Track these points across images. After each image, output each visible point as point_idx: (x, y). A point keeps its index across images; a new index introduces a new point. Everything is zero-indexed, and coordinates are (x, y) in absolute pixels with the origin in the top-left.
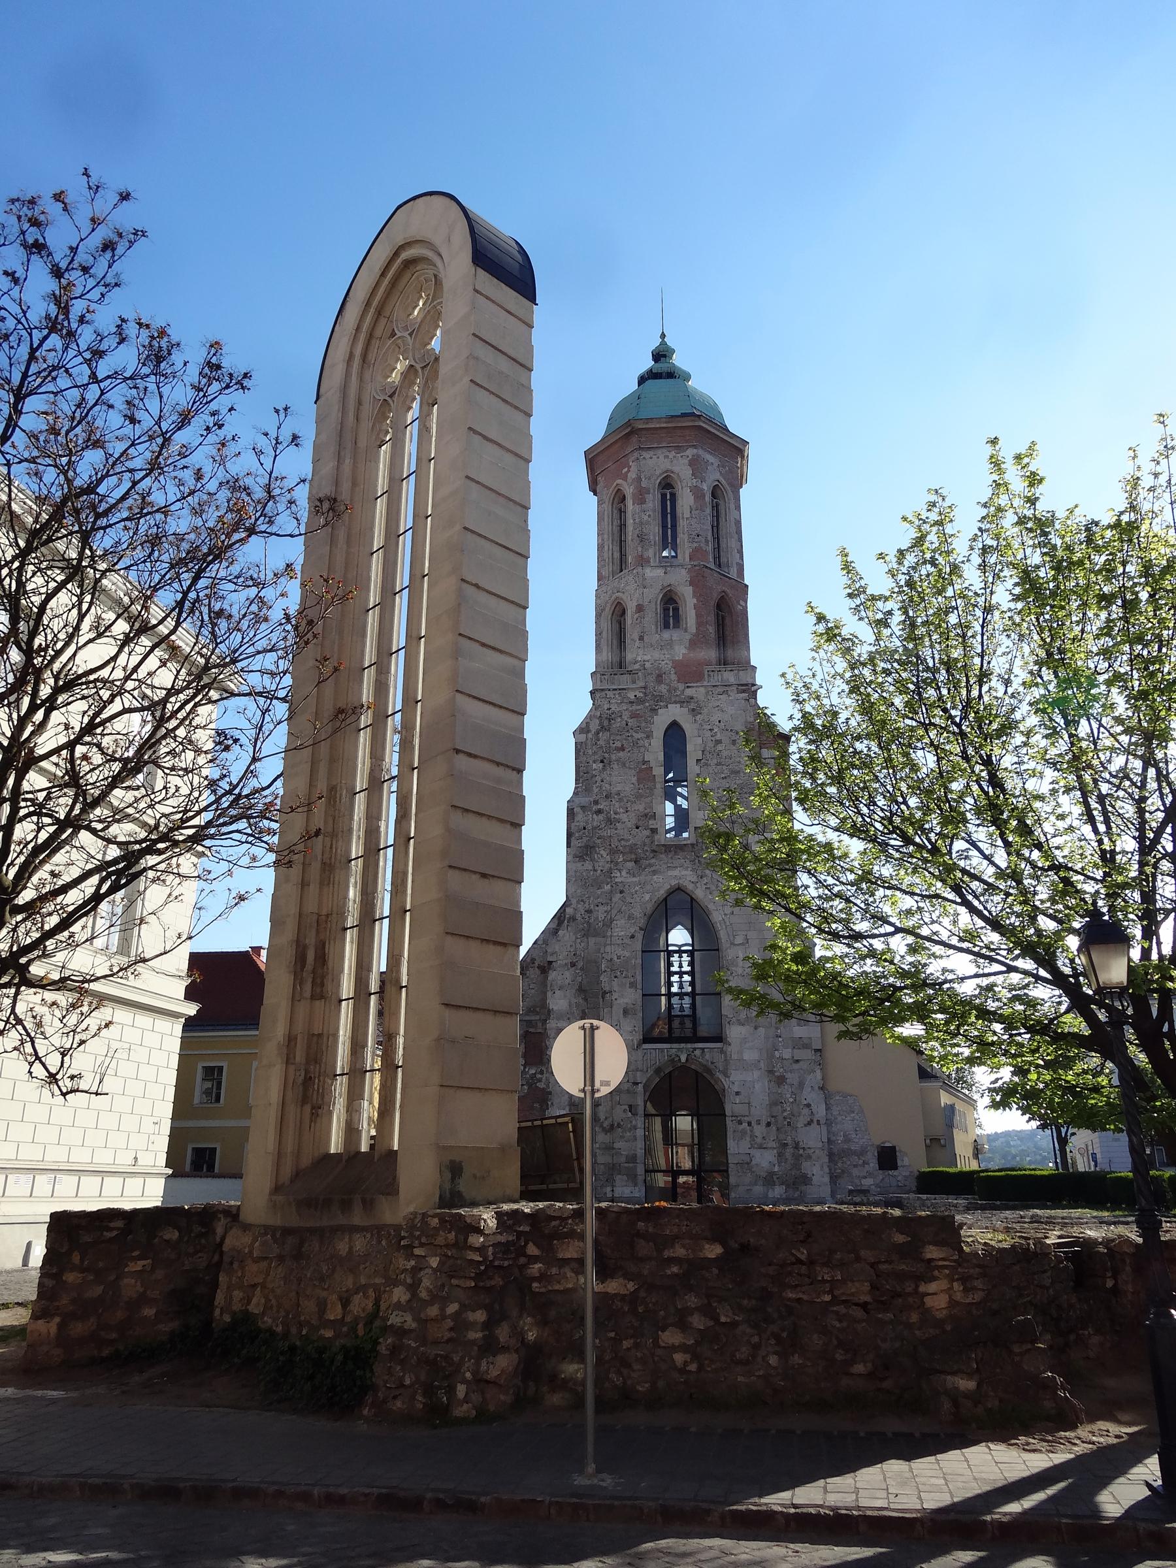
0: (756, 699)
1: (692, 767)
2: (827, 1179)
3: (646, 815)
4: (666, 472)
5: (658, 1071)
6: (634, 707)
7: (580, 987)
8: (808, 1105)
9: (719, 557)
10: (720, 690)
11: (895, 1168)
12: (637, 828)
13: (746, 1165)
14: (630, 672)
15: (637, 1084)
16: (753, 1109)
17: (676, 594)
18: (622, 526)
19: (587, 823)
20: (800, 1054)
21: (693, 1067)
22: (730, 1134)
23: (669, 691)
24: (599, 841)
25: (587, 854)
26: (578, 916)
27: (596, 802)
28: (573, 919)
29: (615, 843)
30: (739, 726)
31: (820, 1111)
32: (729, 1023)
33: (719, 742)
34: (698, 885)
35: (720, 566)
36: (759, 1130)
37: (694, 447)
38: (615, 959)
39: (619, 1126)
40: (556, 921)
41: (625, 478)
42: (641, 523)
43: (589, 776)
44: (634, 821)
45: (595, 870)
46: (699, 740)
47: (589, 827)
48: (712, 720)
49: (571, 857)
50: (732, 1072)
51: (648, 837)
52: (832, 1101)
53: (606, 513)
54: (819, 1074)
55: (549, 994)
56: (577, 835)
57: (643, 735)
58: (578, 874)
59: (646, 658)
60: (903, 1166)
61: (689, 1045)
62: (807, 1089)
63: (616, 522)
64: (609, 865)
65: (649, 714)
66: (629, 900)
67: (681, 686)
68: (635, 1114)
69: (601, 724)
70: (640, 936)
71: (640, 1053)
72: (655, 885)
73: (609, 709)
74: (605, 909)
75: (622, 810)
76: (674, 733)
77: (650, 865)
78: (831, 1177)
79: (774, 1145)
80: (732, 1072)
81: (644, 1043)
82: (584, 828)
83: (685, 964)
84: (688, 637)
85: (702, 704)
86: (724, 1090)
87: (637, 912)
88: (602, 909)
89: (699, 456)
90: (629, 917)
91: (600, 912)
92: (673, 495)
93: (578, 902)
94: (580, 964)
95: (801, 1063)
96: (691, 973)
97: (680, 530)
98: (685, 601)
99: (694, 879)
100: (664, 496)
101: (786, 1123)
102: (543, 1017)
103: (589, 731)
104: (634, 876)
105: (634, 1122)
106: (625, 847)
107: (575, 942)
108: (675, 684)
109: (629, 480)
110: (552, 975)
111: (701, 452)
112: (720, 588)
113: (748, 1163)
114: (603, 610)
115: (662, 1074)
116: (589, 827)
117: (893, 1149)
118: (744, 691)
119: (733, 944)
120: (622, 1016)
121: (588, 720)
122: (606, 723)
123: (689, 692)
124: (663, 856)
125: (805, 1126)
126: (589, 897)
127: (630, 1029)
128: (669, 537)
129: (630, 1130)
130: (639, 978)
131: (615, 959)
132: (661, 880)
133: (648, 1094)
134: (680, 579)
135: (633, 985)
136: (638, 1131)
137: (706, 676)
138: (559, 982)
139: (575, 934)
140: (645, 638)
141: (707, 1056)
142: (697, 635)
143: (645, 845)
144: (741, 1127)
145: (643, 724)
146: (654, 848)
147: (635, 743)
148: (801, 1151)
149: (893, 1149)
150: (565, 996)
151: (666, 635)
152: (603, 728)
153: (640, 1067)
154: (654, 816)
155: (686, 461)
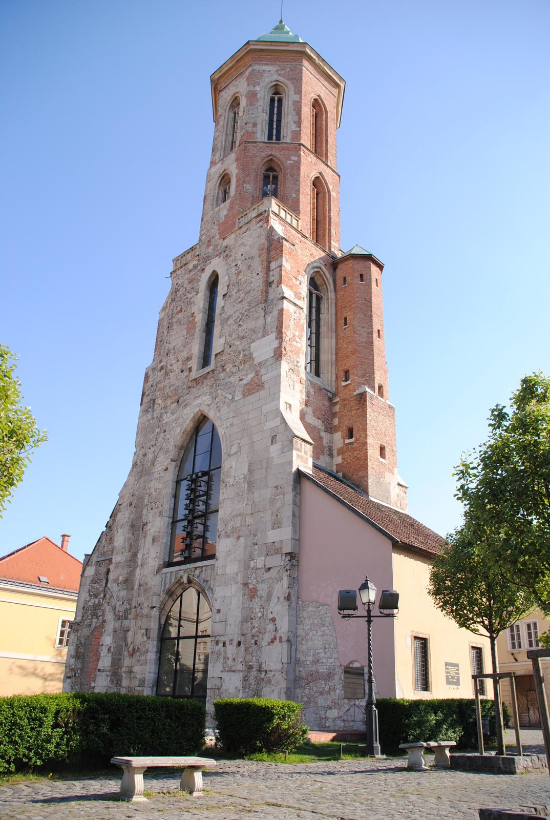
4: (235, 94)
8: (273, 620)
10: (244, 229)
23: (214, 250)
29: (167, 390)
30: (255, 252)
34: (212, 406)
36: (231, 650)
46: (227, 278)
48: (237, 256)
51: (187, 377)
52: (305, 614)
56: (147, 393)
61: (193, 565)
66: (168, 436)
70: (172, 467)
77: (184, 401)
82: (152, 386)
88: (153, 449)
93: (140, 450)
95: (271, 570)
99: (209, 403)
101: (253, 642)
105: (147, 646)
111: (256, 67)
112: (264, 154)
113: (219, 689)
120: (151, 544)
123: (225, 243)
124: (193, 390)
125: (269, 644)
135: (161, 513)
136: (149, 654)
146: (190, 384)
150: (123, 533)
152: (173, 300)
155: (245, 79)
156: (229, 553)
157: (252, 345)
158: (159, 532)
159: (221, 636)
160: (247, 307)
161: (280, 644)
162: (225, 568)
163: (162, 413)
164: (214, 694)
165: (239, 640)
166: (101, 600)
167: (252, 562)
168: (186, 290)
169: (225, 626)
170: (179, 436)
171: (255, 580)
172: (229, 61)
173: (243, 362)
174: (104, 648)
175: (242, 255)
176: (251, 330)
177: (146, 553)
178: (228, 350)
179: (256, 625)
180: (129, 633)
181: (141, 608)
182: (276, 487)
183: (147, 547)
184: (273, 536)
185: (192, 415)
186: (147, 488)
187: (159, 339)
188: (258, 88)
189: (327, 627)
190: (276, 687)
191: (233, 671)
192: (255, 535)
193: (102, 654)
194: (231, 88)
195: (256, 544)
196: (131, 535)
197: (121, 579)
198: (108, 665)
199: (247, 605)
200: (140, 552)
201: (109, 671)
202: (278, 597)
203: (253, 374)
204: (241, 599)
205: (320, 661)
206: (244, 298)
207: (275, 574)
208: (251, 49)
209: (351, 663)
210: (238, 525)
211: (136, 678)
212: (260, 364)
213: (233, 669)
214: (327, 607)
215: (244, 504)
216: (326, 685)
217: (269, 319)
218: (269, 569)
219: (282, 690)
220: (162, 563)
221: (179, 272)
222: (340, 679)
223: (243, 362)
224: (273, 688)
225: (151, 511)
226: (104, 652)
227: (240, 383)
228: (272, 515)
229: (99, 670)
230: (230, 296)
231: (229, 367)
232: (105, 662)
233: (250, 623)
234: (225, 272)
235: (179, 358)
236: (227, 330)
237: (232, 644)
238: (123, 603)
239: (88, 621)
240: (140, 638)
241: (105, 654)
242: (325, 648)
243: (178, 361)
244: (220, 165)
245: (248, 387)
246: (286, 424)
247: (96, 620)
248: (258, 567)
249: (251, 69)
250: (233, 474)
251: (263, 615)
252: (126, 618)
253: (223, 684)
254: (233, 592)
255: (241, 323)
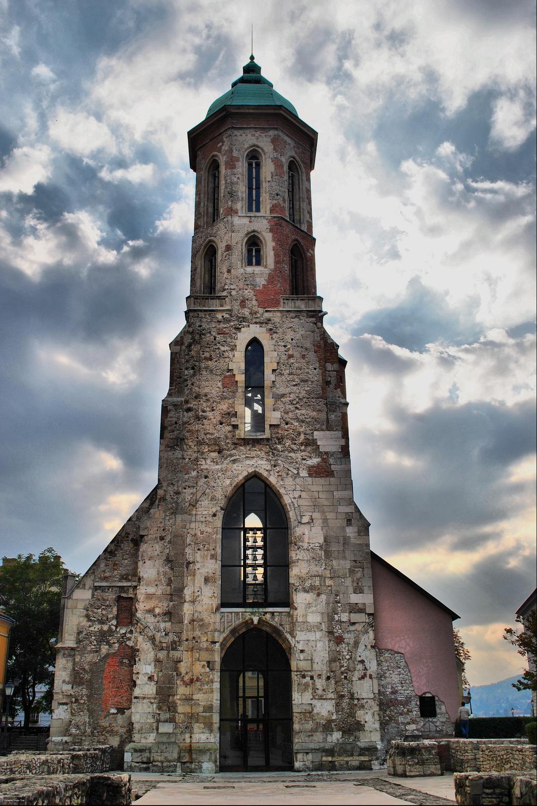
0: (322, 323)
1: (269, 377)
2: (377, 726)
3: (229, 414)
5: (233, 632)
6: (222, 325)
7: (167, 558)
8: (362, 662)
9: (293, 215)
11: (434, 714)
12: (221, 424)
13: (309, 714)
14: (219, 298)
15: (215, 643)
16: (315, 666)
17: (258, 238)
18: (216, 188)
19: (178, 418)
20: (355, 617)
21: (264, 628)
22: (295, 687)
23: (251, 313)
24: (188, 434)
25: (177, 445)
26: (168, 497)
27: (187, 402)
28: (163, 499)
30: (308, 345)
31: (373, 667)
32: (295, 590)
33: (290, 356)
34: (272, 473)
35: (293, 221)
36: (320, 684)
37: (276, 129)
38: (199, 533)
39: (198, 679)
40: (149, 502)
41: (219, 150)
42: (232, 183)
43: (182, 380)
44: (219, 418)
45: (185, 459)
46: (275, 354)
47: (180, 422)
48: (286, 337)
49: (163, 448)
50: (298, 633)
51: (230, 432)
53: (203, 178)
54: (371, 634)
55: (140, 564)
56: (169, 428)
57: (228, 348)
58: (169, 461)
59: (232, 287)
60: (441, 714)
61: (261, 610)
62: (361, 647)
63: (211, 185)
64: (195, 455)
65: (234, 331)
66: (212, 484)
67: (261, 310)
68: (212, 669)
69: (193, 338)
70: (220, 515)
71: (218, 616)
72: (235, 472)
73: (200, 326)
74: (192, 491)
75: (208, 409)
76: (255, 348)
77: (231, 455)
78: (381, 724)
79: (332, 696)
80: (298, 633)
81: (222, 607)
82: (176, 423)
83: (259, 540)
84: (267, 271)
85: (278, 325)
86: (290, 648)
87: (219, 494)
88: (188, 491)
89: (279, 136)
90: (212, 500)
91: (187, 495)
92: (258, 165)
94: (168, 538)
95: (357, 625)
96: (264, 548)
97: (262, 191)
98: (266, 244)
99: (269, 468)
100: (250, 165)
101: (343, 677)
102: (134, 584)
103: (182, 344)
104: (217, 464)
105: (211, 676)
106: (210, 439)
107: (164, 519)
108: (256, 309)
109: (223, 152)
110: (143, 547)
111: (281, 134)
112: (293, 237)
113: (310, 713)
114: (198, 252)
115: (237, 635)
116: (180, 422)
117: (433, 698)
118: (312, 317)
119: (300, 522)
120: (203, 583)
121: (182, 335)
122: (197, 337)
123: (267, 315)
125: (360, 679)
126: (178, 481)
127: (210, 595)
128: (253, 204)
129: (208, 683)
130: (219, 550)
131: (199, 533)
132: (240, 467)
133: (224, 652)
134: (262, 225)
135: (213, 557)
137: (282, 303)
138: (149, 553)
139: (164, 512)
140: (232, 271)
141: (276, 619)
142: (275, 270)
143: (227, 438)
144: (304, 681)
145: (229, 340)
147: (222, 355)
148: (356, 702)
149: (433, 698)
150: (154, 566)
151: (249, 269)
153: (218, 626)
154: (235, 415)
155: (269, 139)
156: (309, 605)
157: (316, 433)
158: (214, 574)
159: (308, 671)
160: (303, 394)
161: (371, 680)
162: (306, 617)
163: (197, 458)
164: (305, 717)
165: (329, 675)
166: (114, 628)
167: (336, 616)
168: (215, 339)
169: (312, 664)
170: (230, 489)
171: (340, 631)
172: (253, 107)
173: (305, 444)
174: (140, 676)
175: (292, 340)
176: (313, 418)
177: (196, 591)
178: (283, 425)
179: (345, 665)
180: (181, 663)
181: (197, 642)
182: (355, 561)
183: (197, 584)
184: (355, 598)
185: (245, 474)
186: (188, 527)
187: (175, 374)
188: (283, 160)
189: (402, 669)
190: (370, 710)
191: (324, 699)
192: (337, 595)
193: (138, 682)
194: (249, 135)
195: (339, 603)
196: (168, 570)
197: (157, 611)
198: (151, 693)
199: (333, 648)
200: (186, 588)
201: (155, 698)
202: (365, 645)
203: (319, 460)
204: (327, 644)
205: (399, 692)
206: (299, 384)
207: (360, 628)
208: (281, 114)
209: (425, 693)
210: (317, 583)
211: (199, 705)
212: (326, 453)
213: (325, 697)
214: (401, 655)
215: (323, 569)
216: (405, 708)
217: (332, 417)
218: (354, 624)
219: (375, 713)
220: (220, 602)
221: (201, 314)
222: (416, 704)
223: (305, 444)
224: (367, 711)
225: (198, 552)
226: (141, 680)
227: (304, 462)
228: (353, 582)
229: (136, 698)
230: (281, 374)
231: (288, 443)
232: (145, 688)
233: (338, 664)
234: (273, 347)
235: (215, 408)
236: (280, 405)
237: (320, 678)
238: (166, 635)
239: (94, 647)
240: (199, 669)
241: (144, 683)
242: (402, 683)
243: (213, 410)
244: (247, 222)
245: (315, 469)
246: (361, 514)
247: (107, 647)
248: (342, 620)
249: (276, 132)
250: (306, 540)
251: (351, 657)
252: (174, 649)
253: (314, 709)
254: (318, 637)
255: (298, 406)
